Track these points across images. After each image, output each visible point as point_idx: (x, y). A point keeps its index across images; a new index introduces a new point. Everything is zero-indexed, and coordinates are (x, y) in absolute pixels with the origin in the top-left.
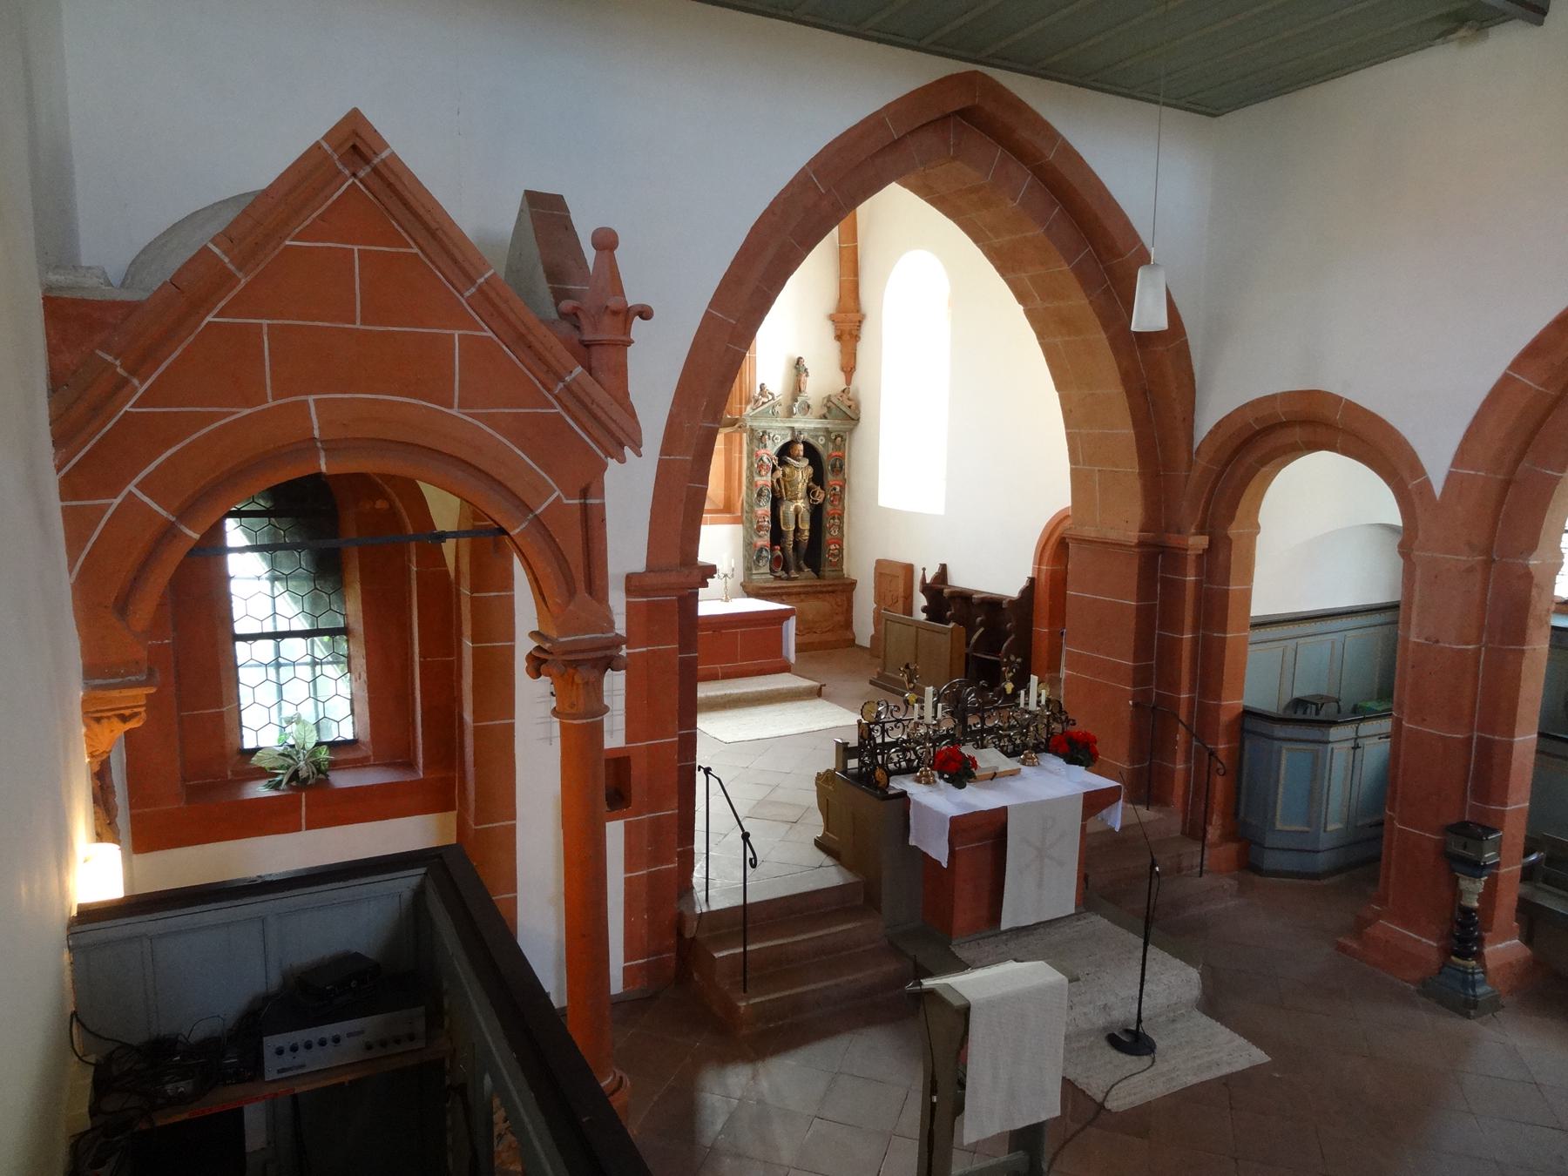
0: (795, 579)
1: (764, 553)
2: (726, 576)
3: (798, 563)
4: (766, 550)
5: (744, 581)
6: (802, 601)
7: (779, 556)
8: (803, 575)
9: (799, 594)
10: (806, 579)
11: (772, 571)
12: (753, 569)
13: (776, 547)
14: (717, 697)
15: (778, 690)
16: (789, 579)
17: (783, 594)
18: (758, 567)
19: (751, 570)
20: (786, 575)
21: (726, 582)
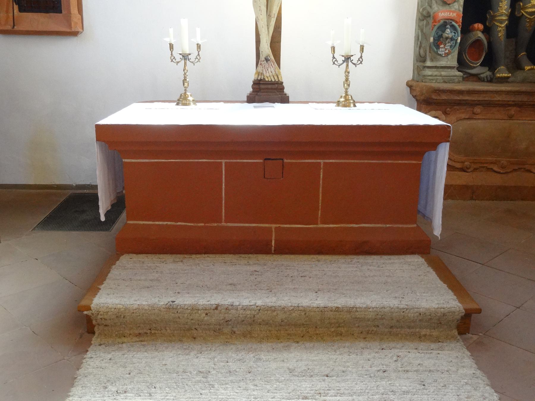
0: (504, 80)
1: (448, 32)
2: (347, 59)
3: (516, 56)
4: (453, 26)
5: (413, 80)
6: (511, 117)
7: (478, 41)
8: (520, 75)
9: (504, 105)
10: (524, 81)
11: (462, 64)
12: (428, 58)
13: (476, 25)
14: (194, 309)
15: (350, 310)
16: (491, 81)
17: (473, 104)
18: (436, 56)
19: (424, 61)
20: (488, 73)
21: (347, 72)
